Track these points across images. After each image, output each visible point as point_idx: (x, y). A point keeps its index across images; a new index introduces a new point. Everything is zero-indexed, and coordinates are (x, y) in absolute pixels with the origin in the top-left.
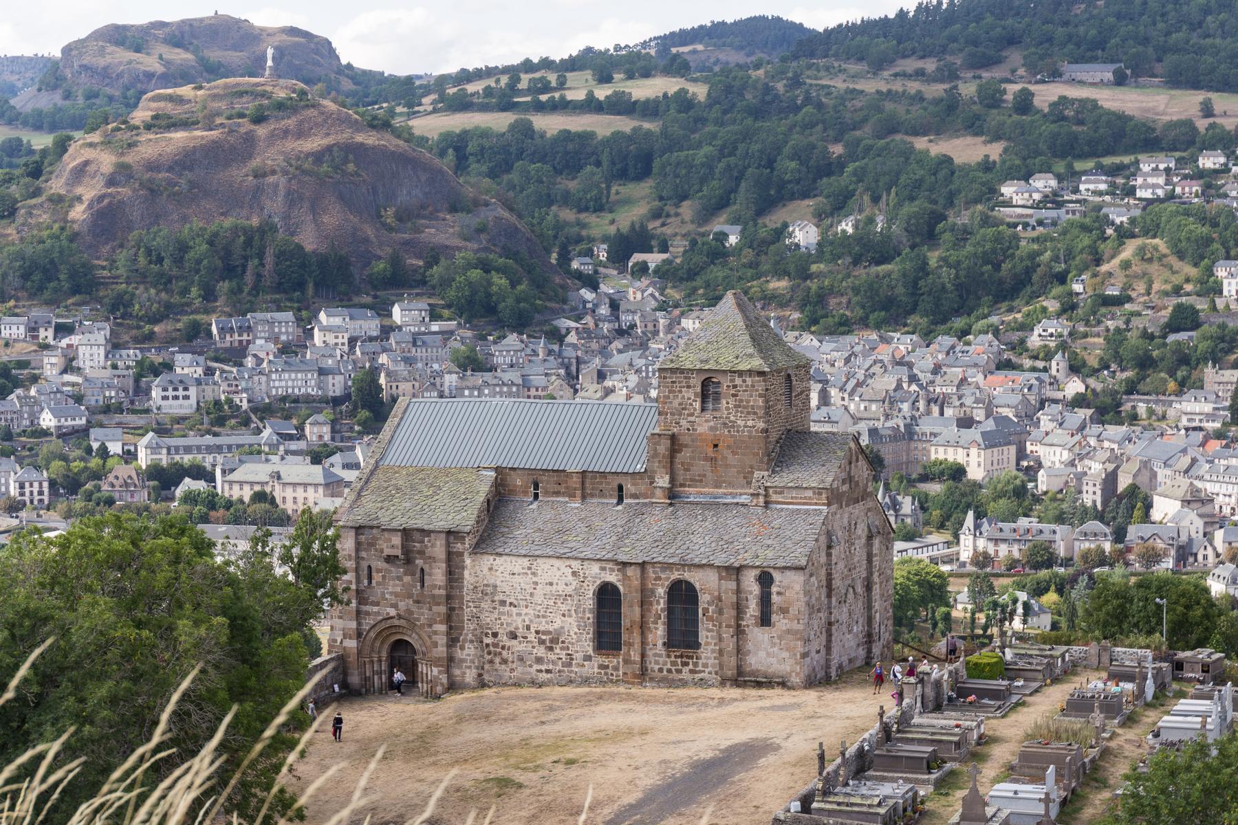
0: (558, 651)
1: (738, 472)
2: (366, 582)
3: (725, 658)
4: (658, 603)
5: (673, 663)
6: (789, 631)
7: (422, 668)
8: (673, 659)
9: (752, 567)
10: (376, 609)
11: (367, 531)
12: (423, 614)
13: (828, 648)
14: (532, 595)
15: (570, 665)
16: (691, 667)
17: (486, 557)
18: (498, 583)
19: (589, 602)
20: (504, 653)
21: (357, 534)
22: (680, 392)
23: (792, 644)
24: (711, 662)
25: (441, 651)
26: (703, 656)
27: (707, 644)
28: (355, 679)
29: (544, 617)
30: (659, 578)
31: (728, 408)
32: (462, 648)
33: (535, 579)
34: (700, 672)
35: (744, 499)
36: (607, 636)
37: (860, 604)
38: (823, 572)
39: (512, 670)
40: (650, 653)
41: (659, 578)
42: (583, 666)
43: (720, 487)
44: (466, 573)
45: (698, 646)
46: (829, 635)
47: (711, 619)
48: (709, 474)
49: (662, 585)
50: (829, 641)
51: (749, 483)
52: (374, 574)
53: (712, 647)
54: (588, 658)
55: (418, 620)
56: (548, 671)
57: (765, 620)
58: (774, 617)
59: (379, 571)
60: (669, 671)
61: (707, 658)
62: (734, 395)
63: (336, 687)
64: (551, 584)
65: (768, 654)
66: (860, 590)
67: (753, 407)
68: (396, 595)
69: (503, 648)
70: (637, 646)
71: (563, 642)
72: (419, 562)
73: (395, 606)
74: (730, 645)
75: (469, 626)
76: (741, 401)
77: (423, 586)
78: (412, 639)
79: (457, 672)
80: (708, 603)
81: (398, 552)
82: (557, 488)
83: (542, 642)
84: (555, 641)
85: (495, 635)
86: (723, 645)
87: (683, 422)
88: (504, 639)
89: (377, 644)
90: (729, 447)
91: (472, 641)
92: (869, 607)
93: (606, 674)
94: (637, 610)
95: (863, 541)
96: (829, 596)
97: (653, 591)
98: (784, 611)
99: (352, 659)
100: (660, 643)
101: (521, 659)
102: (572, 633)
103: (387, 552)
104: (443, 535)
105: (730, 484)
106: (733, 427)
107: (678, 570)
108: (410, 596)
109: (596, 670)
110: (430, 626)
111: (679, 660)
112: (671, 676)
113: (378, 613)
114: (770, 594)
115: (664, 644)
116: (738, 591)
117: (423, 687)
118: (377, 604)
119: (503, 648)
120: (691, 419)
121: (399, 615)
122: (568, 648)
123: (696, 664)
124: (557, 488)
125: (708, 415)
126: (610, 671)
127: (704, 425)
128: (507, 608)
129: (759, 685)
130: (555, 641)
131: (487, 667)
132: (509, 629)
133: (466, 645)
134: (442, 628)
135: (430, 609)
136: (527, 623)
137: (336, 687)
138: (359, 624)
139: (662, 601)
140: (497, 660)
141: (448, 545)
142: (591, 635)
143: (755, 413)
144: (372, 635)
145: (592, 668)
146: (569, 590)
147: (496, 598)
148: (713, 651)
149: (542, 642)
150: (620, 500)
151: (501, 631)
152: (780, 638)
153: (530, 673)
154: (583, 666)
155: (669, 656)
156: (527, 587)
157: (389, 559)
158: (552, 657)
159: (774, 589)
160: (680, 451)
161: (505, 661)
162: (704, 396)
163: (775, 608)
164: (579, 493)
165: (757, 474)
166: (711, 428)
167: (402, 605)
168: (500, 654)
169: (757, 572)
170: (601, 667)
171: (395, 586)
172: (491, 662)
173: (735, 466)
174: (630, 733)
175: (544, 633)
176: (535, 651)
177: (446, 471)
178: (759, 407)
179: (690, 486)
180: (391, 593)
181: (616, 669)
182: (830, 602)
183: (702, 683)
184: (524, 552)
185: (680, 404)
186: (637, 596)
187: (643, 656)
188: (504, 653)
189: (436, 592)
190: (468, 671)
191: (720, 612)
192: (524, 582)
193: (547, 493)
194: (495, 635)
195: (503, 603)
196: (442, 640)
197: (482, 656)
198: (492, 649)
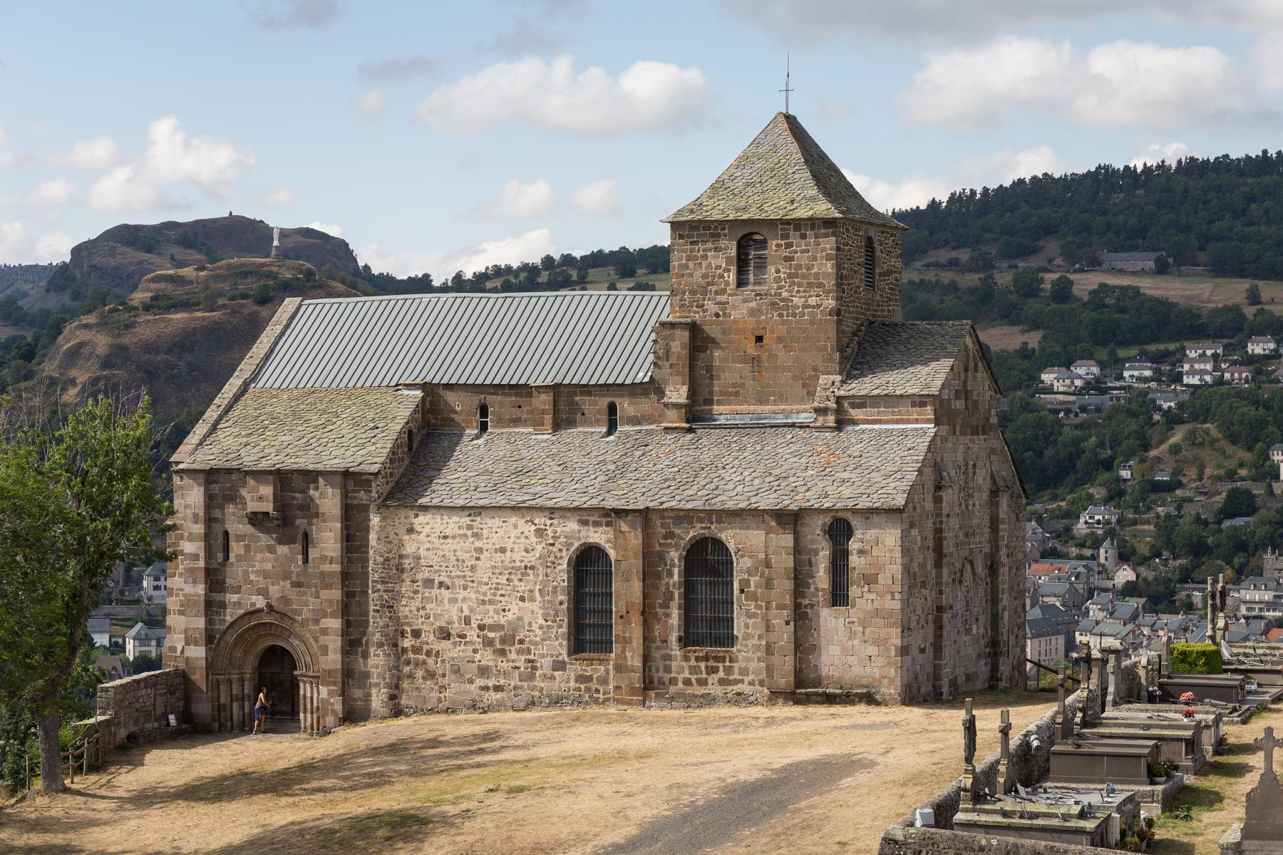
0: (513, 656)
1: (795, 378)
2: (220, 556)
3: (776, 659)
4: (670, 574)
5: (694, 670)
6: (877, 613)
7: (305, 689)
8: (693, 663)
9: (821, 511)
11: (222, 477)
13: (938, 648)
14: (473, 568)
15: (532, 677)
16: (721, 674)
17: (402, 513)
18: (422, 552)
19: (561, 575)
20: (431, 661)
22: (705, 257)
23: (883, 633)
24: (753, 665)
25: (333, 659)
26: (741, 656)
27: (747, 637)
28: (203, 709)
29: (491, 602)
30: (671, 535)
31: (777, 280)
32: (365, 656)
33: (478, 544)
34: (737, 682)
35: (804, 418)
36: (587, 629)
37: (981, 593)
38: (929, 524)
39: (443, 688)
40: (657, 655)
41: (671, 535)
42: (552, 678)
43: (766, 402)
44: (373, 537)
45: (730, 640)
46: (939, 627)
47: (753, 597)
48: (749, 383)
49: (677, 546)
50: (938, 636)
51: (811, 394)
52: (233, 544)
53: (755, 641)
54: (559, 666)
55: (299, 612)
56: (498, 688)
57: (839, 596)
58: (854, 591)
59: (239, 538)
60: (687, 682)
61: (748, 660)
62: (787, 259)
63: (172, 719)
64: (503, 550)
65: (844, 651)
66: (980, 570)
67: (817, 275)
68: (266, 575)
69: (429, 653)
70: (637, 643)
71: (521, 642)
73: (263, 592)
74: (784, 635)
75: (376, 624)
76: (799, 267)
77: (306, 561)
78: (294, 646)
79: (358, 693)
80: (749, 572)
81: (268, 507)
82: (516, 413)
83: (488, 643)
84: (508, 640)
85: (416, 634)
86: (773, 637)
87: (711, 306)
88: (429, 638)
89: (238, 654)
90: (780, 339)
91: (380, 645)
92: (994, 600)
93: (588, 690)
94: (637, 586)
95: (985, 496)
96: (938, 565)
97: (661, 557)
98: (870, 580)
99: (199, 678)
100: (673, 638)
101: (457, 671)
102: (535, 627)
103: (252, 506)
104: (338, 479)
105: (782, 399)
106: (787, 308)
107: (701, 520)
108: (286, 576)
109: (572, 684)
110: (317, 621)
111: (703, 665)
112: (689, 691)
113: (239, 603)
114: (846, 554)
115: (680, 639)
116: (798, 550)
117: (305, 718)
118: (237, 590)
119: (429, 653)
120: (723, 298)
121: (270, 607)
122: (529, 652)
123: (729, 670)
124: (516, 413)
125: (748, 291)
126: (594, 686)
127: (740, 308)
128: (435, 591)
129: (830, 699)
130: (508, 640)
131: (405, 685)
132: (438, 624)
133: (372, 650)
134: (335, 624)
135: (317, 597)
136: (466, 612)
137: (172, 719)
138: (209, 622)
139: (676, 571)
140: (420, 673)
141: (345, 495)
142: (564, 630)
143: (820, 285)
144: (231, 638)
145: (566, 681)
146: (532, 558)
147: (420, 576)
148: (757, 648)
149: (488, 643)
150: (612, 428)
151: (425, 627)
152: (864, 624)
153: (470, 692)
154: (552, 678)
155: (686, 659)
156: (465, 556)
157: (257, 520)
158: (505, 665)
159: (853, 545)
160: (704, 349)
161: (431, 675)
162: (742, 263)
163: (854, 576)
164: (548, 418)
165: (823, 379)
166: (752, 312)
167: (275, 591)
168: (424, 663)
169: (828, 519)
170: (581, 679)
171: (262, 562)
172: (411, 676)
173: (789, 369)
174: (622, 756)
175: (493, 628)
176: (478, 657)
177: (349, 393)
178: (827, 275)
179: (719, 403)
180: (258, 572)
181: (604, 681)
182: (939, 575)
183: (740, 699)
184: (460, 502)
185: (705, 276)
186: (636, 564)
187: (646, 658)
188: (431, 661)
189: (327, 567)
191: (768, 584)
192: (463, 548)
193: (500, 422)
194: (416, 634)
195: (429, 583)
196: (334, 643)
197: (397, 668)
198: (411, 656)
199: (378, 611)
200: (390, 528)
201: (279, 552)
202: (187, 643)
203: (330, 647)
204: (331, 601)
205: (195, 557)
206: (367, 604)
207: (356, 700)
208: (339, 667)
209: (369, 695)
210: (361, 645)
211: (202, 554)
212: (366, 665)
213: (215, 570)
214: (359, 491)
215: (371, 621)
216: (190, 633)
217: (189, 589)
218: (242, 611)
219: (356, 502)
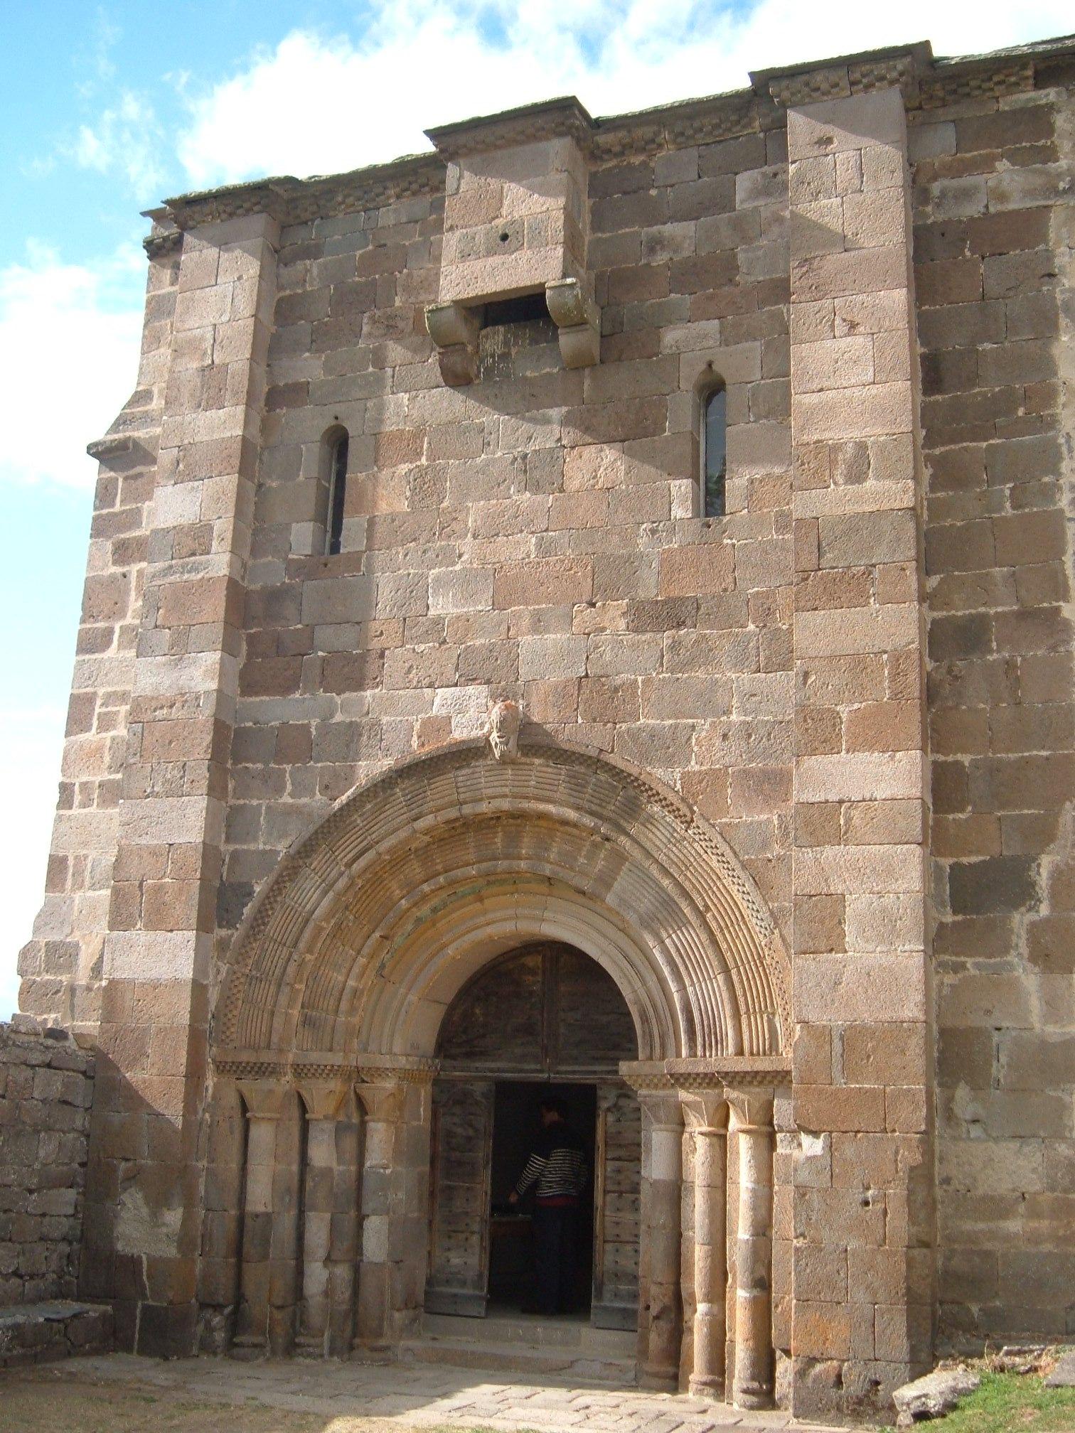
2: (303, 537)
21: (279, 256)
55: (671, 747)
68: (507, 589)
72: (690, 339)
81: (538, 266)
99: (157, 1077)
104: (888, 101)
110: (772, 784)
134: (888, 776)
138: (229, 821)
144: (314, 896)
171: (491, 532)
189: (835, 500)
196: (882, 888)
201: (575, 481)
202: (120, 918)
203: (857, 905)
204: (858, 664)
205: (195, 539)
207: (997, 1207)
208: (911, 1008)
211: (223, 526)
213: (274, 596)
214: (986, 164)
216: (133, 870)
217: (150, 677)
219: (972, 210)
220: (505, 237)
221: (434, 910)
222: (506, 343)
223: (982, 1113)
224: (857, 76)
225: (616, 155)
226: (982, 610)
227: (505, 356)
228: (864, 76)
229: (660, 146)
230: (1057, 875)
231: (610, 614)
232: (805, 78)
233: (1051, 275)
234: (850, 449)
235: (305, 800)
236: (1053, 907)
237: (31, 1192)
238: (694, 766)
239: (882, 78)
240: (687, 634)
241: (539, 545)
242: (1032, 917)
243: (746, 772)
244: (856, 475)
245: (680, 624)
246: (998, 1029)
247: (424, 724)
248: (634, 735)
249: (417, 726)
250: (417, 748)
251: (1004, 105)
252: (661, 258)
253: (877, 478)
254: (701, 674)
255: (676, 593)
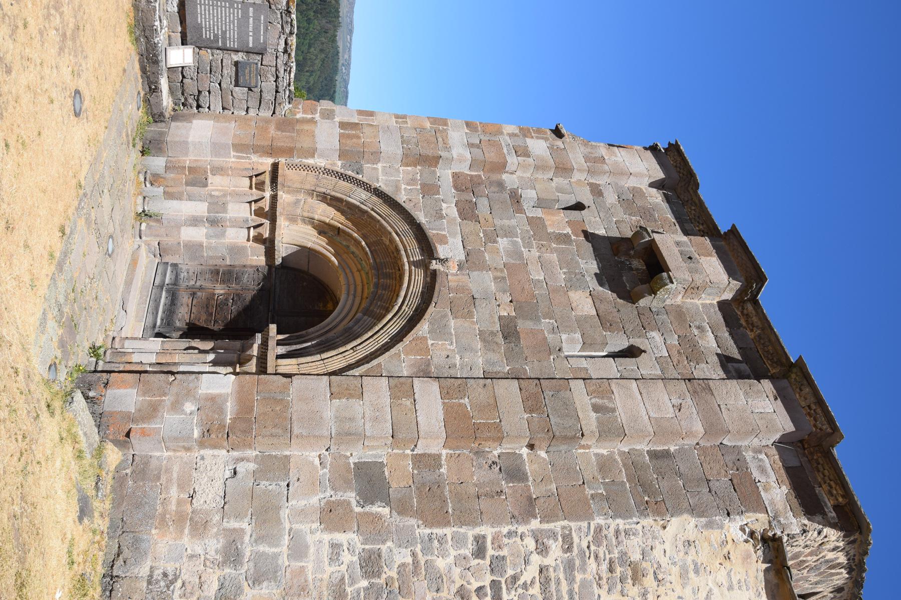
10: (450, 209)
12: (464, 349)
55: (439, 331)
68: (515, 268)
91: (371, 564)
113: (439, 216)
118: (467, 212)
167: (482, 282)
171: (543, 264)
190: (213, 545)
199: (480, 552)
200: (722, 576)
206: (496, 521)
209: (200, 527)
210: (367, 498)
212: (301, 514)
215: (448, 531)
218: (421, 217)
220: (690, 258)
221: (353, 253)
222: (637, 269)
223: (239, 476)
224: (813, 407)
225: (742, 312)
226: (531, 479)
227: (631, 269)
228: (815, 410)
229: (752, 330)
230: (379, 517)
231: (508, 308)
232: (805, 382)
233: (728, 514)
234: (611, 405)
235: (403, 193)
236: (359, 514)
237: (220, 84)
238: (430, 342)
239: (815, 420)
240: (500, 339)
241: (539, 281)
242: (354, 503)
243: (428, 365)
244: (596, 408)
245: (505, 338)
246: (288, 485)
247: (445, 236)
248: (445, 316)
249: (444, 233)
250: (431, 232)
251: (817, 490)
252: (696, 332)
253: (597, 418)
254: (479, 345)
255: (522, 336)
